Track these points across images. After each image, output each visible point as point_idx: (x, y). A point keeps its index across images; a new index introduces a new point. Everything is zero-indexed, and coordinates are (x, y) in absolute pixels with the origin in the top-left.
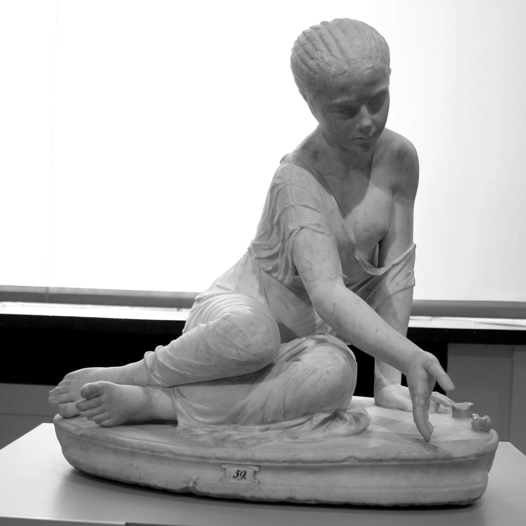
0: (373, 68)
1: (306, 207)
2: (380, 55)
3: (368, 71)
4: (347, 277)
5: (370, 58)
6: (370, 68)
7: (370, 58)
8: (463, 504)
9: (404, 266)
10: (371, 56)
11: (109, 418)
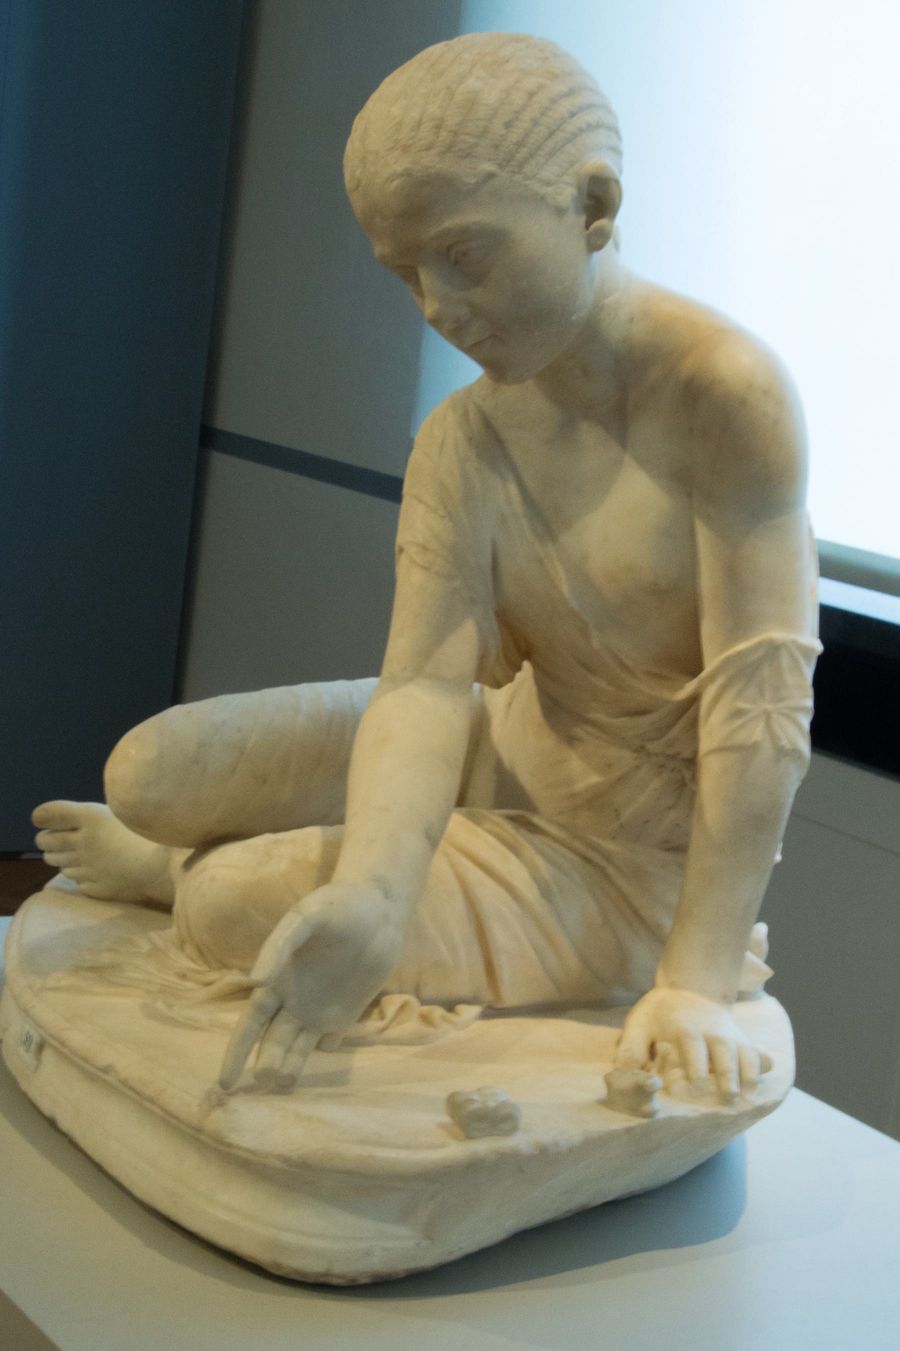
0: (407, 174)
1: (420, 501)
2: (441, 138)
3: (396, 183)
4: (611, 689)
5: (406, 149)
6: (401, 175)
7: (406, 149)
8: (335, 1281)
9: (724, 688)
10: (410, 142)
11: (94, 881)
